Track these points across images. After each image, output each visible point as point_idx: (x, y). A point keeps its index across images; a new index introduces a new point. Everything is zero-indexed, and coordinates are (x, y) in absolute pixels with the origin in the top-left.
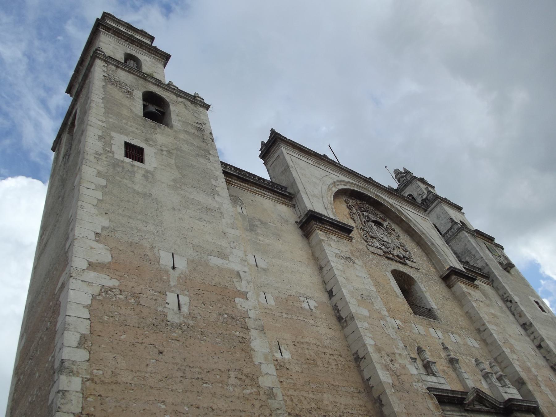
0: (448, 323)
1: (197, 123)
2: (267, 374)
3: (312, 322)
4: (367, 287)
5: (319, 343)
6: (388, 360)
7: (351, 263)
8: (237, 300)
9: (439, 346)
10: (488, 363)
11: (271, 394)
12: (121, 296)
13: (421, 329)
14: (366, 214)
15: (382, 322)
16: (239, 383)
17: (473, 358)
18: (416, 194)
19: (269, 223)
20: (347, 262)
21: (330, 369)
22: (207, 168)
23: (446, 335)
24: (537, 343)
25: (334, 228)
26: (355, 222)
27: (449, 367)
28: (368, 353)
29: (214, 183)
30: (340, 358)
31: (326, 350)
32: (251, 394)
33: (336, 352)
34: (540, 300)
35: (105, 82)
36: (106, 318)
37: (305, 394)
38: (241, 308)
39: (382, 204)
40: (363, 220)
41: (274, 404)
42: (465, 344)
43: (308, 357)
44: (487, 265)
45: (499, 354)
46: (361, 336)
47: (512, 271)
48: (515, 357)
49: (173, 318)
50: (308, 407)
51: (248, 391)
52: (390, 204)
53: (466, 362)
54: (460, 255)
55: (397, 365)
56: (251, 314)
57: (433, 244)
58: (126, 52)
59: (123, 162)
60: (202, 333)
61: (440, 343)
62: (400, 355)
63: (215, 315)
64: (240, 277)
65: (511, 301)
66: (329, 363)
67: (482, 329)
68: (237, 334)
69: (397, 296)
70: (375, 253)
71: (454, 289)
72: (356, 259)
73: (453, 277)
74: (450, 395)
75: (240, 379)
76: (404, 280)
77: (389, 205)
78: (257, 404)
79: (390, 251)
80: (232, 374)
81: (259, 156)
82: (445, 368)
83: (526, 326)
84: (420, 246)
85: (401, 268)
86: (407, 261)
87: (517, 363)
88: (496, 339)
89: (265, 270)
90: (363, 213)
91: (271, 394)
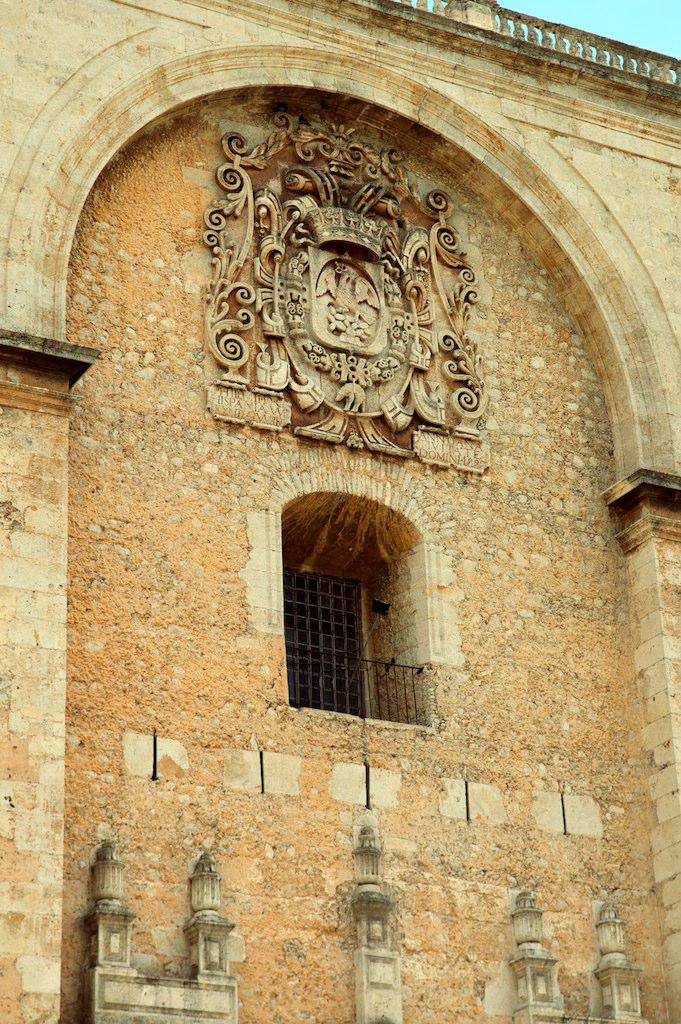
0: (484, 732)
4: (23, 636)
9: (343, 839)
10: (597, 904)
13: (286, 772)
14: (306, 205)
17: (517, 885)
23: (424, 790)
26: (213, 265)
39: (438, 138)
40: (266, 251)
42: (523, 828)
45: (671, 874)
52: (489, 133)
53: (453, 905)
57: (640, 335)
61: (357, 830)
67: (659, 760)
69: (246, 629)
70: (241, 426)
71: (636, 561)
72: (43, 502)
73: (647, 512)
77: (481, 135)
79: (344, 401)
85: (362, 480)
86: (425, 443)
90: (295, 203)
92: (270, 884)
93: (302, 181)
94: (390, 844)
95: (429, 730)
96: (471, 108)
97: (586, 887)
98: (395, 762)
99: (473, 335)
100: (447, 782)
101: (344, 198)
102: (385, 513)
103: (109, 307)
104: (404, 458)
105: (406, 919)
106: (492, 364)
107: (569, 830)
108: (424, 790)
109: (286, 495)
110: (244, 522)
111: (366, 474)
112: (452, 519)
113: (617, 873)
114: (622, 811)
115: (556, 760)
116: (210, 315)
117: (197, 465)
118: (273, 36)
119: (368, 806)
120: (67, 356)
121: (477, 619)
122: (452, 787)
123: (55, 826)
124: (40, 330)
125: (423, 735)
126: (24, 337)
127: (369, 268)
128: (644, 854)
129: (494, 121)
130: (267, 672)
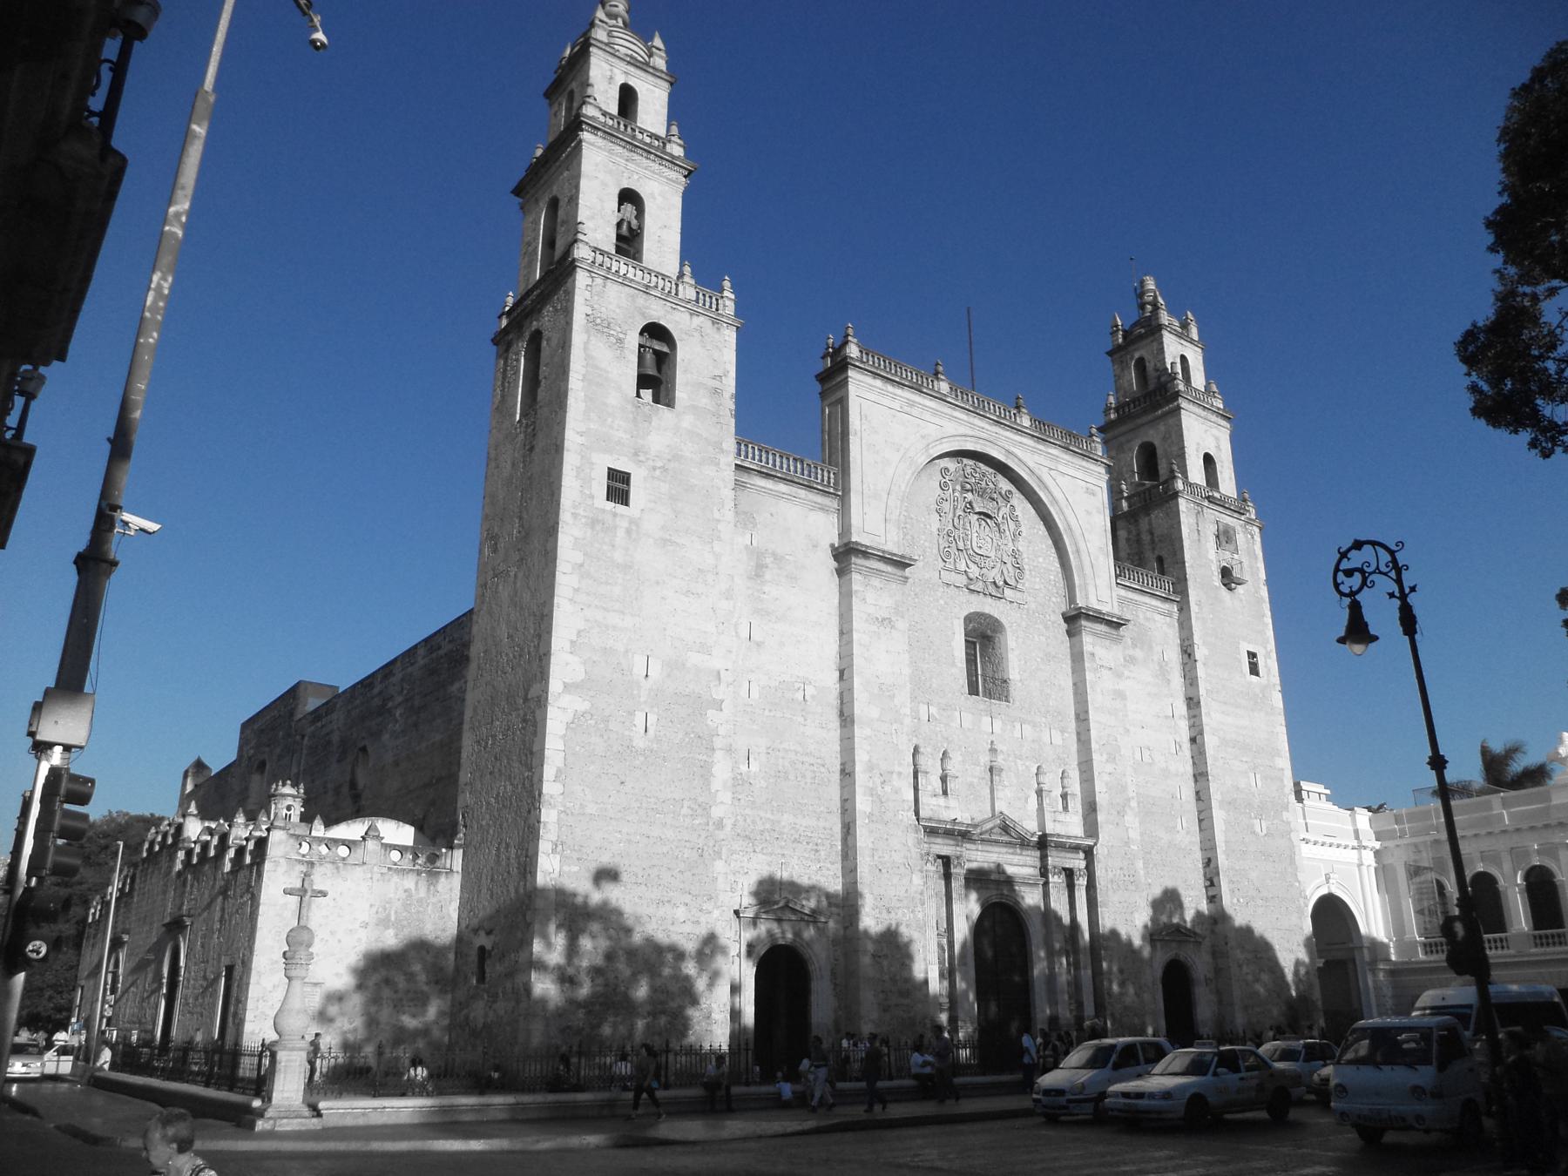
1: (714, 378)
2: (722, 803)
3: (801, 719)
5: (799, 749)
6: (878, 780)
7: (888, 630)
8: (710, 712)
11: (720, 825)
12: (592, 722)
13: (968, 719)
15: (895, 726)
16: (691, 812)
18: (1152, 364)
19: (787, 557)
20: (882, 628)
21: (802, 784)
22: (713, 486)
24: (1193, 735)
25: (885, 563)
27: (983, 778)
28: (854, 772)
29: (717, 515)
30: (823, 770)
31: (805, 759)
32: (700, 824)
33: (819, 761)
34: (1265, 648)
35: (587, 332)
36: (578, 748)
37: (762, 814)
38: (711, 723)
41: (721, 835)
43: (780, 768)
44: (1186, 579)
46: (854, 749)
47: (1240, 589)
48: (1109, 768)
49: (640, 742)
50: (762, 828)
51: (697, 822)
54: (1156, 539)
55: (888, 788)
56: (721, 731)
57: (1078, 551)
58: (622, 187)
59: (604, 511)
60: (664, 759)
62: (900, 774)
63: (680, 735)
64: (720, 679)
65: (1189, 655)
66: (804, 776)
67: (1082, 717)
68: (700, 757)
69: (953, 664)
75: (692, 809)
78: (704, 834)
80: (686, 804)
81: (816, 376)
82: (976, 780)
83: (1193, 703)
87: (1106, 778)
88: (1090, 740)
89: (759, 645)
91: (720, 825)
92: (964, 761)
94: (998, 746)
96: (1025, 460)
99: (1020, 548)
101: (982, 494)
103: (909, 537)
105: (1004, 774)
106: (1026, 560)
109: (966, 613)
110: (952, 623)
116: (941, 541)
117: (938, 601)
118: (963, 430)
121: (1023, 662)
123: (909, 740)
124: (895, 551)
126: (895, 555)
127: (988, 521)
129: (1031, 464)
130: (961, 682)
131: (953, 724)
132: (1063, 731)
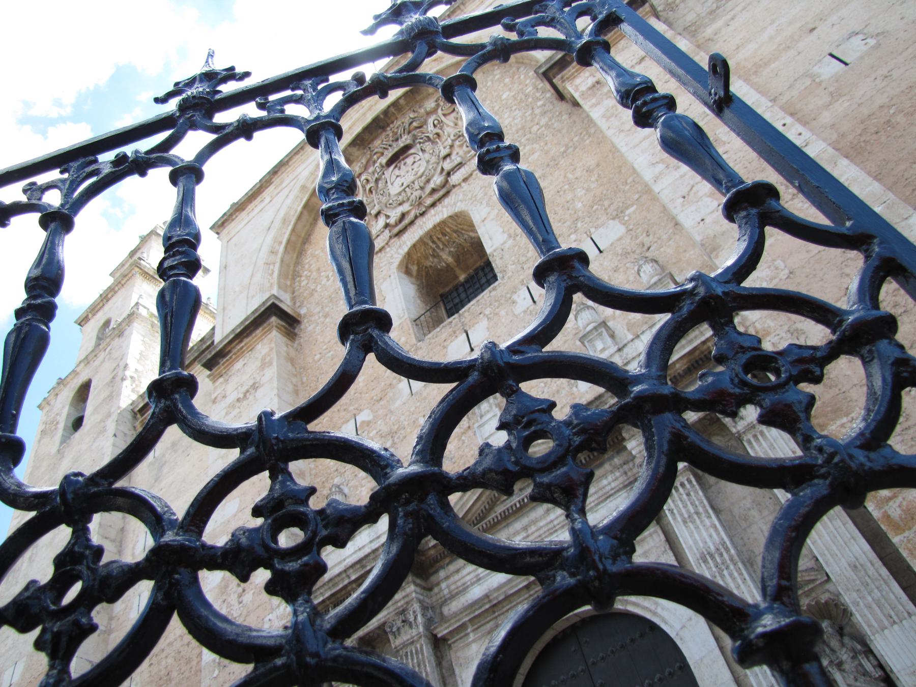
74: (353, 577)
76: (456, 232)
84: (522, 63)
86: (455, 179)
93: (375, 157)
95: (496, 283)
97: (628, 265)
98: (482, 315)
100: (515, 297)
102: (450, 221)
104: (447, 194)
107: (601, 249)
108: (503, 313)
111: (432, 216)
112: (481, 188)
113: (645, 240)
114: (635, 207)
115: (579, 225)
119: (472, 350)
120: (263, 309)
122: (519, 296)
125: (494, 289)
127: (412, 151)
128: (661, 213)
131: (398, 403)
132: (618, 216)
